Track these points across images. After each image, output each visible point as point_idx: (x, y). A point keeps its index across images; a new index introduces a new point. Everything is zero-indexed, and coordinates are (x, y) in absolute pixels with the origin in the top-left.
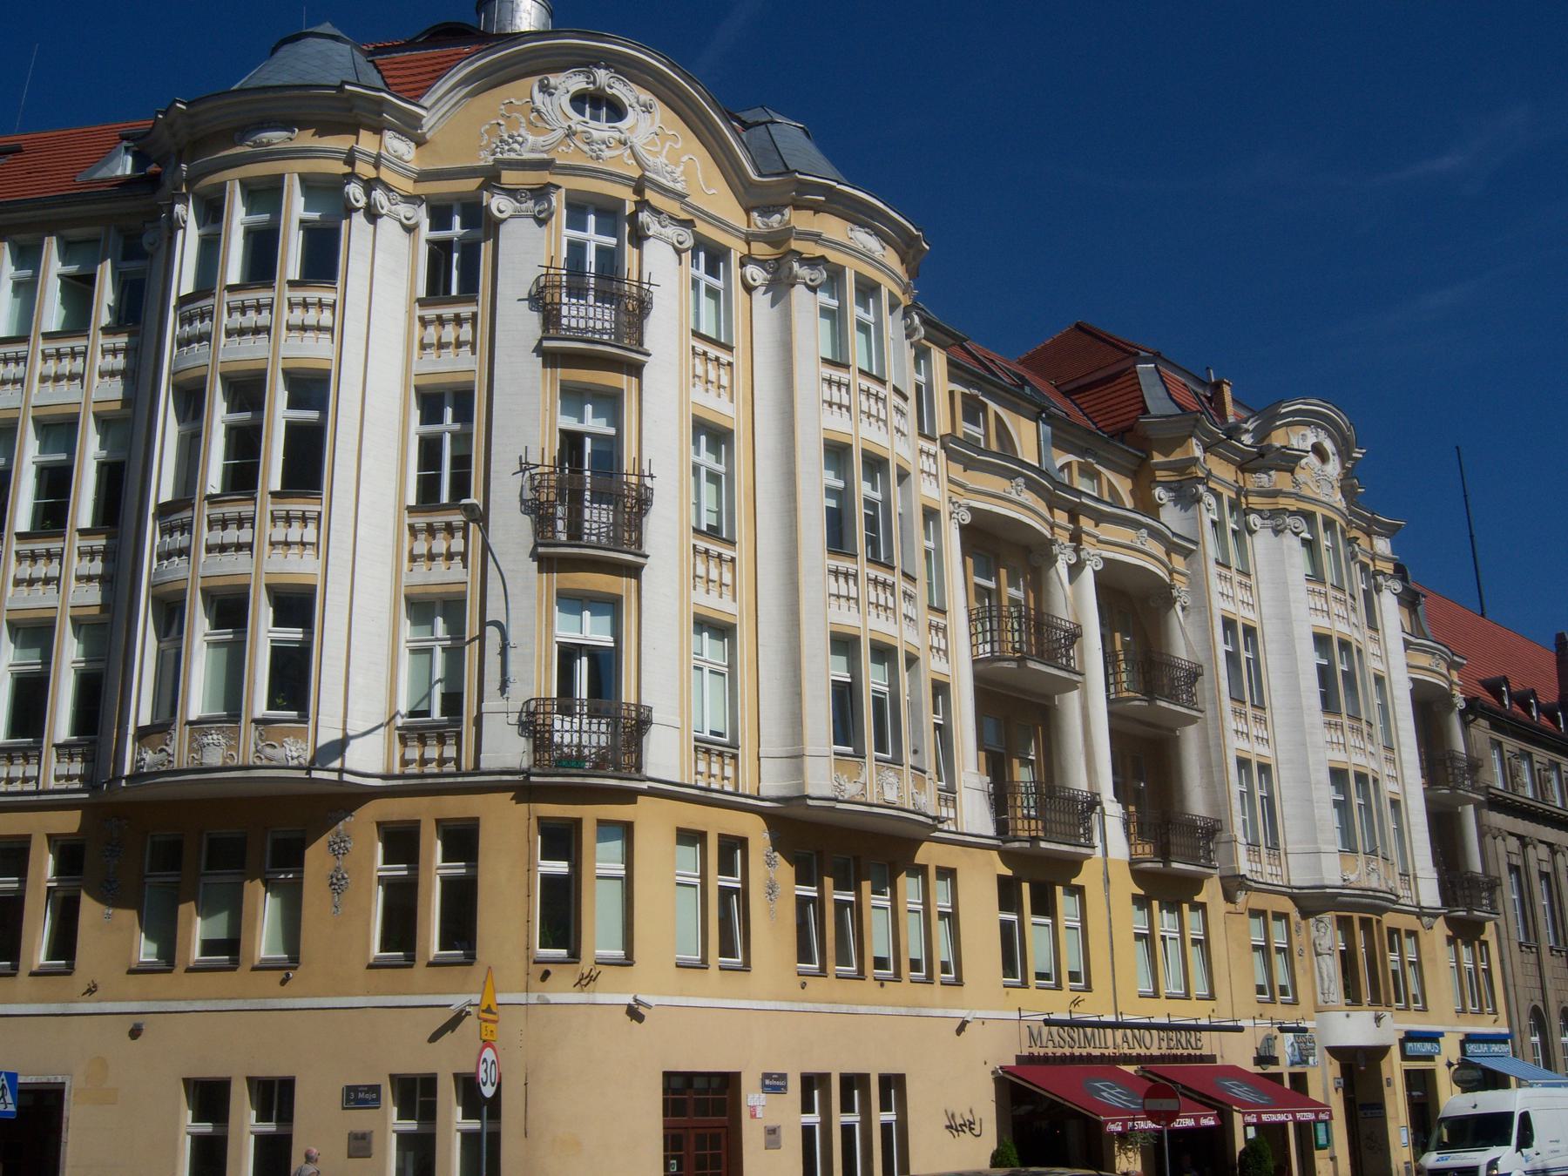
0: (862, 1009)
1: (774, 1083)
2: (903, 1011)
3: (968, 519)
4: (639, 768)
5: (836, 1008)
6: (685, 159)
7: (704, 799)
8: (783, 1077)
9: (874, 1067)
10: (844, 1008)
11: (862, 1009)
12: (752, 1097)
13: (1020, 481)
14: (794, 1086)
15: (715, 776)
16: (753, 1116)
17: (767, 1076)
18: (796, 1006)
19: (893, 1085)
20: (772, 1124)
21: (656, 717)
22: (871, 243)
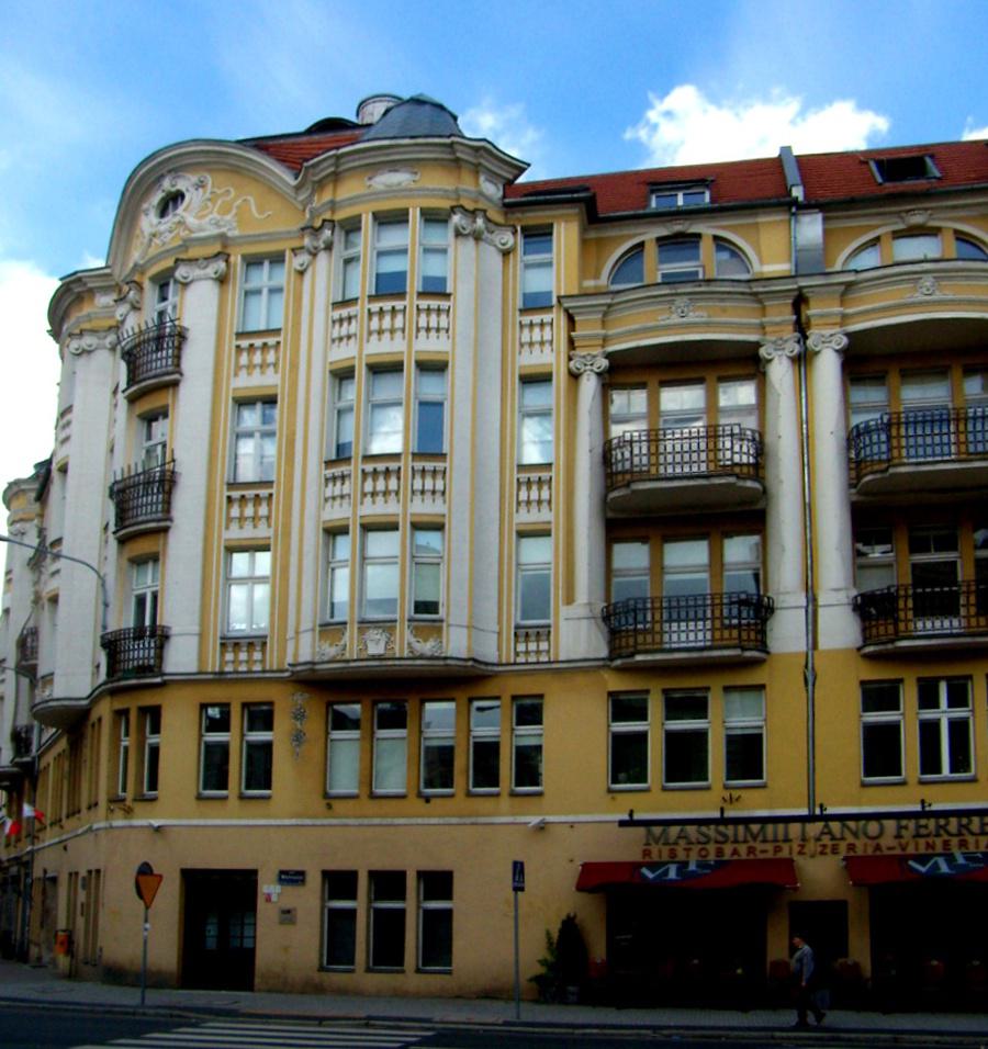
0: (397, 821)
1: (292, 878)
2: (454, 820)
3: (604, 363)
4: (160, 667)
5: (366, 821)
6: (239, 202)
7: (220, 678)
8: (302, 873)
9: (411, 862)
10: (376, 821)
11: (397, 821)
12: (268, 887)
13: (680, 301)
14: (314, 881)
15: (241, 661)
16: (268, 898)
17: (282, 872)
18: (318, 822)
19: (438, 883)
20: (287, 907)
21: (174, 630)
22: (400, 178)
